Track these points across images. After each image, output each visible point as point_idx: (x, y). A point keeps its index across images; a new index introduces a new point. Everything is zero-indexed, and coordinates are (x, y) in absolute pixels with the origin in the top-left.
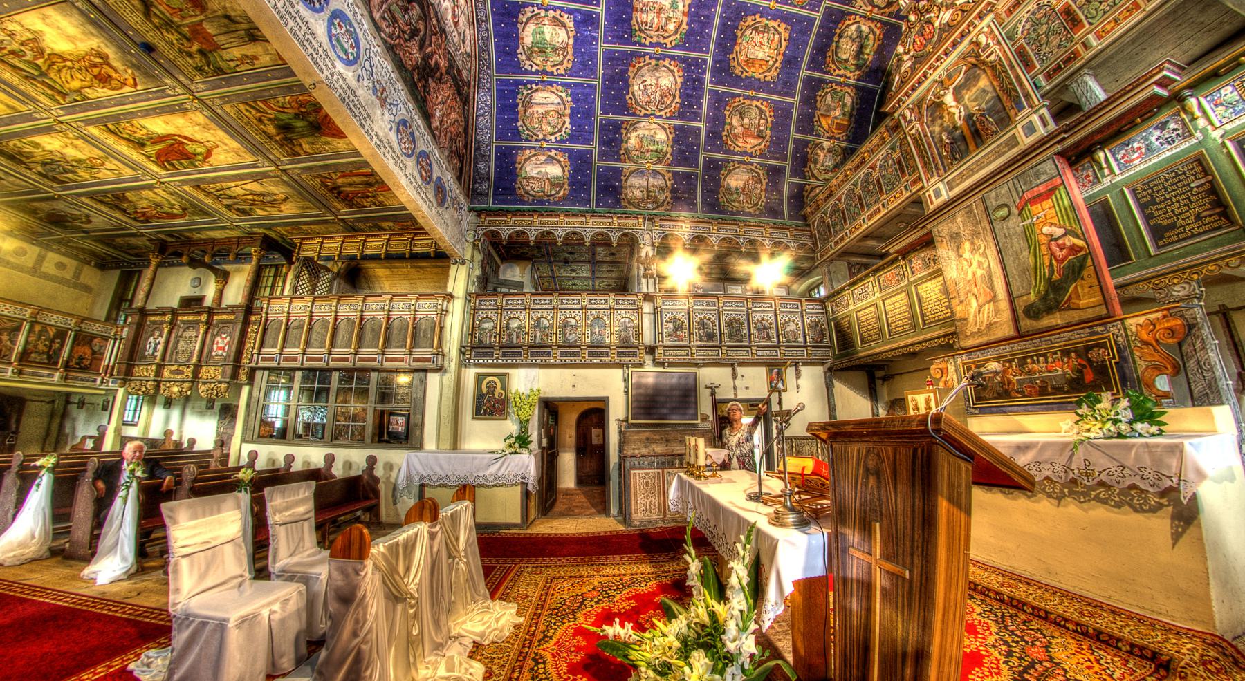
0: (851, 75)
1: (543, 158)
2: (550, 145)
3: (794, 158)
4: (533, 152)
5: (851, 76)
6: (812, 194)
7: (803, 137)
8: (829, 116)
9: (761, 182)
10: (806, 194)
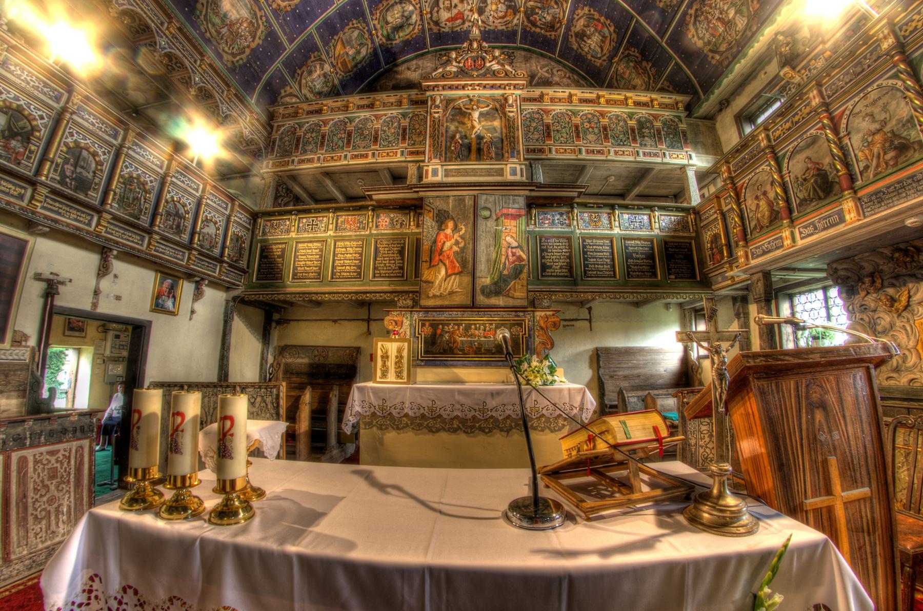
0: (380, 37)
3: (299, 48)
5: (379, 39)
6: (288, 99)
7: (317, 39)
8: (345, 48)
9: (254, 37)
10: (283, 94)
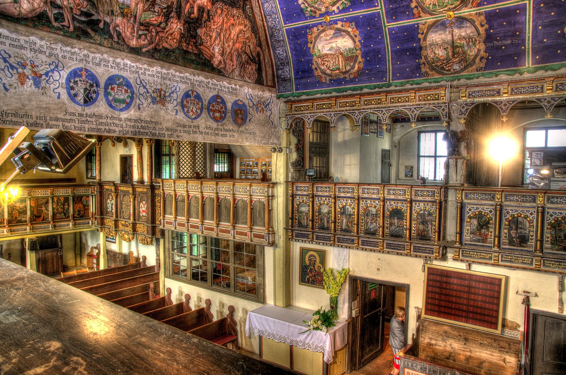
1: (332, 32)
2: (334, 17)
4: (321, 29)
